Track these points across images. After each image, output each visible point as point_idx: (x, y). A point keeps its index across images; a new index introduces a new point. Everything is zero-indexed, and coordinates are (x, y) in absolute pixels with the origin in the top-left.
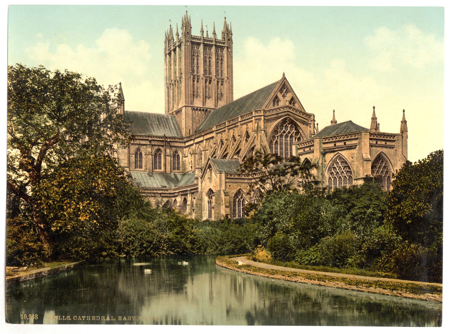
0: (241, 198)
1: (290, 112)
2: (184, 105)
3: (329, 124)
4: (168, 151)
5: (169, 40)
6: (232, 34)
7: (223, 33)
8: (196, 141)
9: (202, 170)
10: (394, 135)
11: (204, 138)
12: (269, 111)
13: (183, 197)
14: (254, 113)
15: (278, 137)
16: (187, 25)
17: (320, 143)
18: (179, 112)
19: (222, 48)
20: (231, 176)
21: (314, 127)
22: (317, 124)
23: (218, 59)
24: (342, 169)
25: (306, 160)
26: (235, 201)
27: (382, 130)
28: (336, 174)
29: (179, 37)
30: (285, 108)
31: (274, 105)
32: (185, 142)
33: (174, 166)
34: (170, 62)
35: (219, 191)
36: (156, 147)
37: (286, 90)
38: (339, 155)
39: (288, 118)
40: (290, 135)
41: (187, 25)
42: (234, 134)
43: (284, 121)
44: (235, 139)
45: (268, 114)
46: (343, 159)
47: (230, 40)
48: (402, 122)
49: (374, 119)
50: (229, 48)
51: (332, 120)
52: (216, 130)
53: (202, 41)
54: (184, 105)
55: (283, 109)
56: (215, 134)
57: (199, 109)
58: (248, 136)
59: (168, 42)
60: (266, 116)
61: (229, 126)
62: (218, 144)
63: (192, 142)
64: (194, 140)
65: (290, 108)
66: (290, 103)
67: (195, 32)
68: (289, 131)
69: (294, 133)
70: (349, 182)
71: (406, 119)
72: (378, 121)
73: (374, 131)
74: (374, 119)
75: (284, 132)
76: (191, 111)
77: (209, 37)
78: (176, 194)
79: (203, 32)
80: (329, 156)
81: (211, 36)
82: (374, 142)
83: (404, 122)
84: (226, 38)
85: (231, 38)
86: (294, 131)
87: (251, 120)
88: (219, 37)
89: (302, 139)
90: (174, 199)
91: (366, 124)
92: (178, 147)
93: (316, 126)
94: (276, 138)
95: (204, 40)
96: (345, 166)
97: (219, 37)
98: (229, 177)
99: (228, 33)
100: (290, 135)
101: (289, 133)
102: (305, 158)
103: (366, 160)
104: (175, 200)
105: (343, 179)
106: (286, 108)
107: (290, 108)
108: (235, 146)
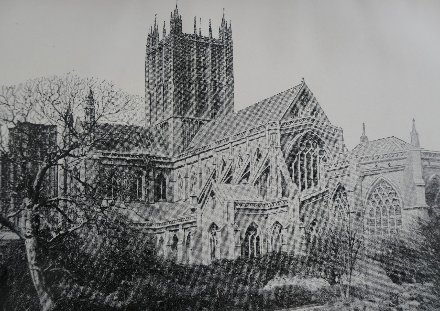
0: (255, 234)
1: (313, 125)
2: (172, 115)
4: (151, 173)
5: (153, 36)
6: (231, 33)
8: (188, 161)
9: (198, 199)
11: (199, 156)
12: (287, 124)
13: (173, 234)
14: (267, 126)
15: (298, 156)
17: (357, 163)
18: (164, 125)
19: (221, 48)
20: (241, 206)
25: (339, 185)
26: (247, 239)
28: (379, 203)
29: (167, 35)
30: (302, 121)
33: (309, 162)
34: (153, 63)
35: (292, 224)
36: (137, 169)
37: (307, 99)
39: (310, 134)
40: (313, 153)
42: (224, 158)
43: (305, 137)
44: (242, 160)
45: (284, 127)
46: (388, 184)
52: (215, 147)
54: (171, 116)
55: (304, 121)
56: (214, 152)
57: (191, 120)
58: (259, 155)
59: (151, 41)
60: (283, 130)
61: (250, 136)
62: (219, 165)
63: (182, 163)
64: (185, 159)
65: (313, 120)
66: (312, 114)
68: (312, 150)
69: (318, 152)
70: (396, 213)
75: (305, 151)
76: (181, 123)
78: (163, 230)
80: (369, 180)
81: (205, 34)
86: (318, 149)
87: (227, 146)
88: (216, 35)
89: (327, 160)
90: (159, 236)
92: (164, 169)
94: (296, 157)
95: (198, 38)
96: (391, 193)
97: (216, 35)
98: (238, 207)
100: (313, 153)
101: (312, 151)
102: (337, 182)
103: (418, 186)
104: (161, 238)
105: (381, 211)
106: (308, 120)
107: (313, 120)
108: (243, 167)
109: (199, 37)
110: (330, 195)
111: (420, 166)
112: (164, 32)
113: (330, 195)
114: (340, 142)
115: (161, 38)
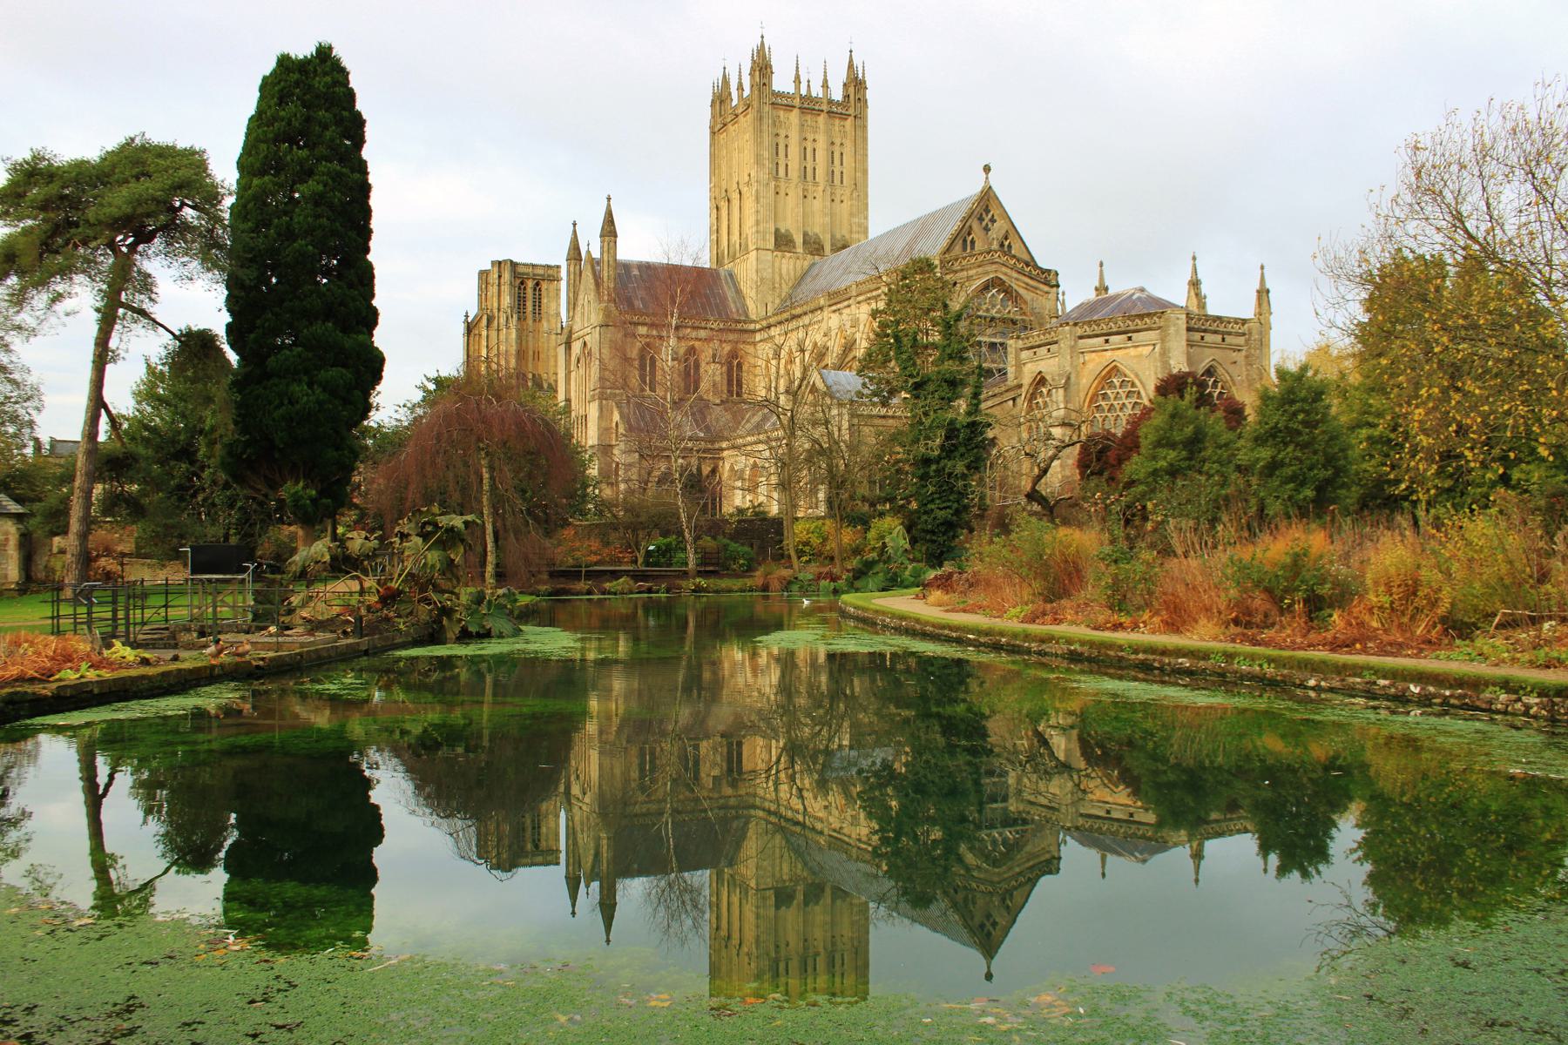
3: (1091, 295)
5: (720, 98)
7: (845, 85)
10: (1244, 321)
16: (762, 67)
21: (1058, 299)
22: (1063, 294)
23: (833, 143)
24: (1124, 396)
27: (1212, 310)
29: (747, 92)
31: (964, 249)
32: (754, 332)
41: (762, 67)
47: (862, 101)
48: (1258, 292)
49: (1195, 284)
50: (860, 118)
51: (1097, 284)
53: (797, 102)
67: (782, 82)
71: (1268, 286)
72: (1204, 289)
73: (1194, 309)
74: (1195, 284)
77: (814, 94)
79: (797, 80)
81: (817, 91)
82: (1197, 336)
83: (1263, 293)
84: (852, 97)
85: (864, 95)
91: (1178, 295)
93: (1060, 297)
97: (837, 94)
99: (856, 84)
109: (808, 98)
110: (1024, 390)
111: (1184, 343)
112: (740, 87)
113: (1024, 390)
115: (735, 102)
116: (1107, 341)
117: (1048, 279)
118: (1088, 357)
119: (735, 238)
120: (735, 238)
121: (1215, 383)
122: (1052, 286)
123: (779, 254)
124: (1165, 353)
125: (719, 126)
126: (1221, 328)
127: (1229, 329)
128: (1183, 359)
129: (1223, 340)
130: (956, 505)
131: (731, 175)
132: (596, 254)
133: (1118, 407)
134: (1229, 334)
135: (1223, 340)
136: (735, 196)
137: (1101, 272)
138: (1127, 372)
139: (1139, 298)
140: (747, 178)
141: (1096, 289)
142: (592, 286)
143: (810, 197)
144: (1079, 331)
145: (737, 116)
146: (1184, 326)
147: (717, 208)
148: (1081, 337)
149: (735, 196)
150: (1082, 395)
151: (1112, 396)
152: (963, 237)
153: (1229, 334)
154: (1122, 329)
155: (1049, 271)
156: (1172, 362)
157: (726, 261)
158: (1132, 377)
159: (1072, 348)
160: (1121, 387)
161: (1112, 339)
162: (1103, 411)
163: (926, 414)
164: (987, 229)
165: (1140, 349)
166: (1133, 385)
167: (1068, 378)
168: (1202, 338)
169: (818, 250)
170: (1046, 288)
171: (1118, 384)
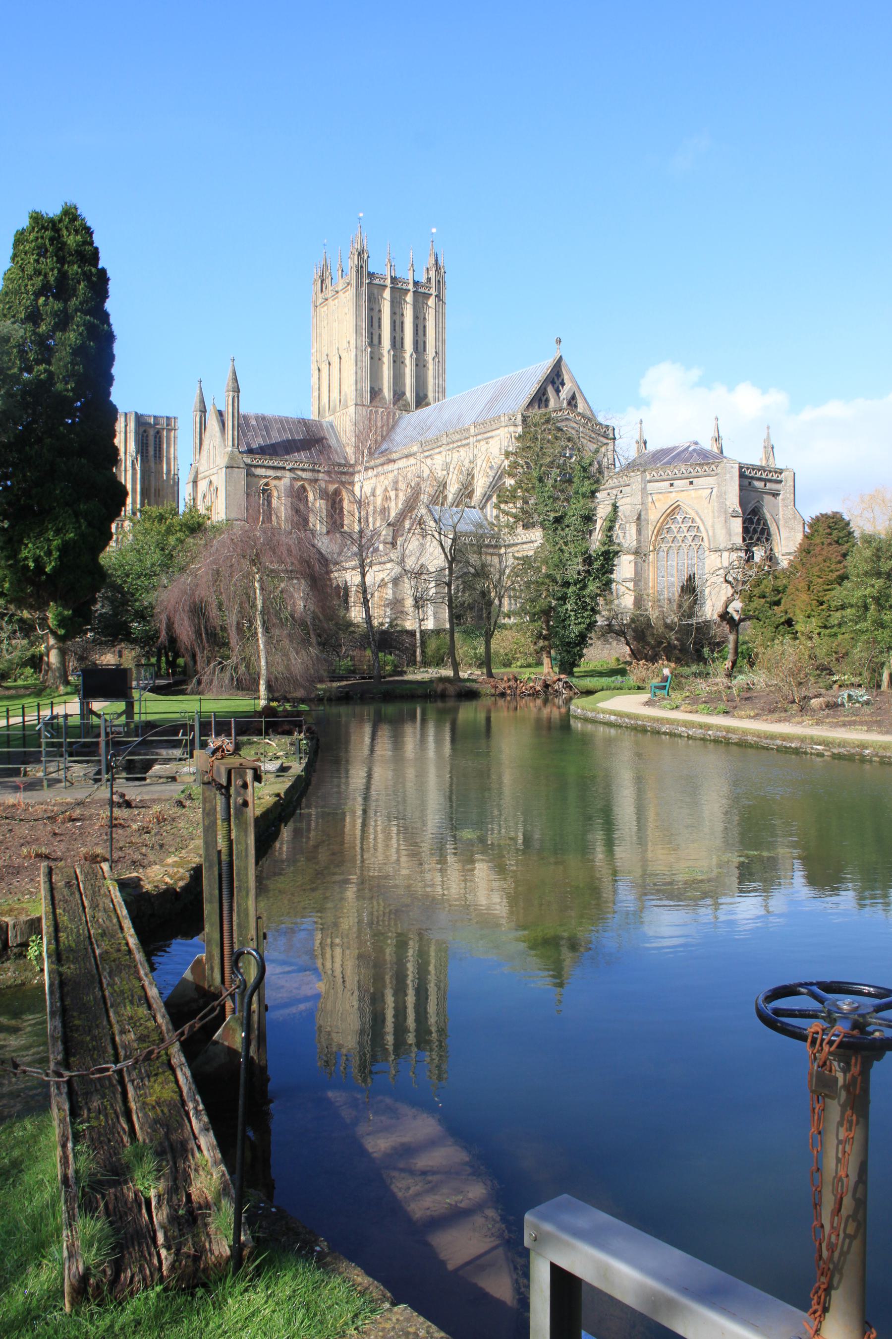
38: (679, 506)
111: (737, 488)
114: (610, 447)
116: (672, 485)
117: (606, 434)
118: (655, 497)
119: (335, 394)
120: (335, 394)
121: (758, 519)
122: (610, 439)
123: (374, 410)
124: (722, 496)
125: (320, 301)
126: (764, 476)
127: (769, 477)
128: (736, 500)
129: (765, 485)
130: (588, 620)
131: (331, 342)
132: (222, 408)
133: (680, 539)
134: (770, 481)
135: (765, 485)
136: (335, 360)
137: (641, 428)
138: (689, 511)
139: (694, 450)
140: (345, 345)
141: (637, 442)
142: (218, 434)
143: (398, 363)
144: (648, 477)
145: (337, 292)
146: (738, 474)
147: (319, 370)
148: (650, 482)
149: (335, 360)
150: (651, 528)
151: (675, 530)
152: (539, 398)
153: (770, 481)
154: (686, 475)
155: (607, 427)
156: (728, 503)
157: (327, 414)
158: (693, 514)
159: (644, 489)
160: (683, 522)
161: (675, 482)
162: (668, 542)
163: (566, 544)
164: (558, 391)
165: (700, 492)
166: (693, 521)
167: (640, 515)
168: (750, 483)
169: (404, 406)
170: (605, 441)
171: (680, 520)
